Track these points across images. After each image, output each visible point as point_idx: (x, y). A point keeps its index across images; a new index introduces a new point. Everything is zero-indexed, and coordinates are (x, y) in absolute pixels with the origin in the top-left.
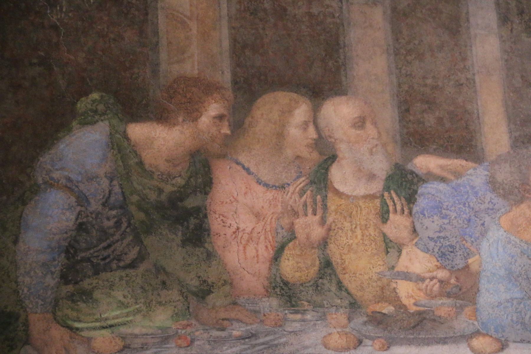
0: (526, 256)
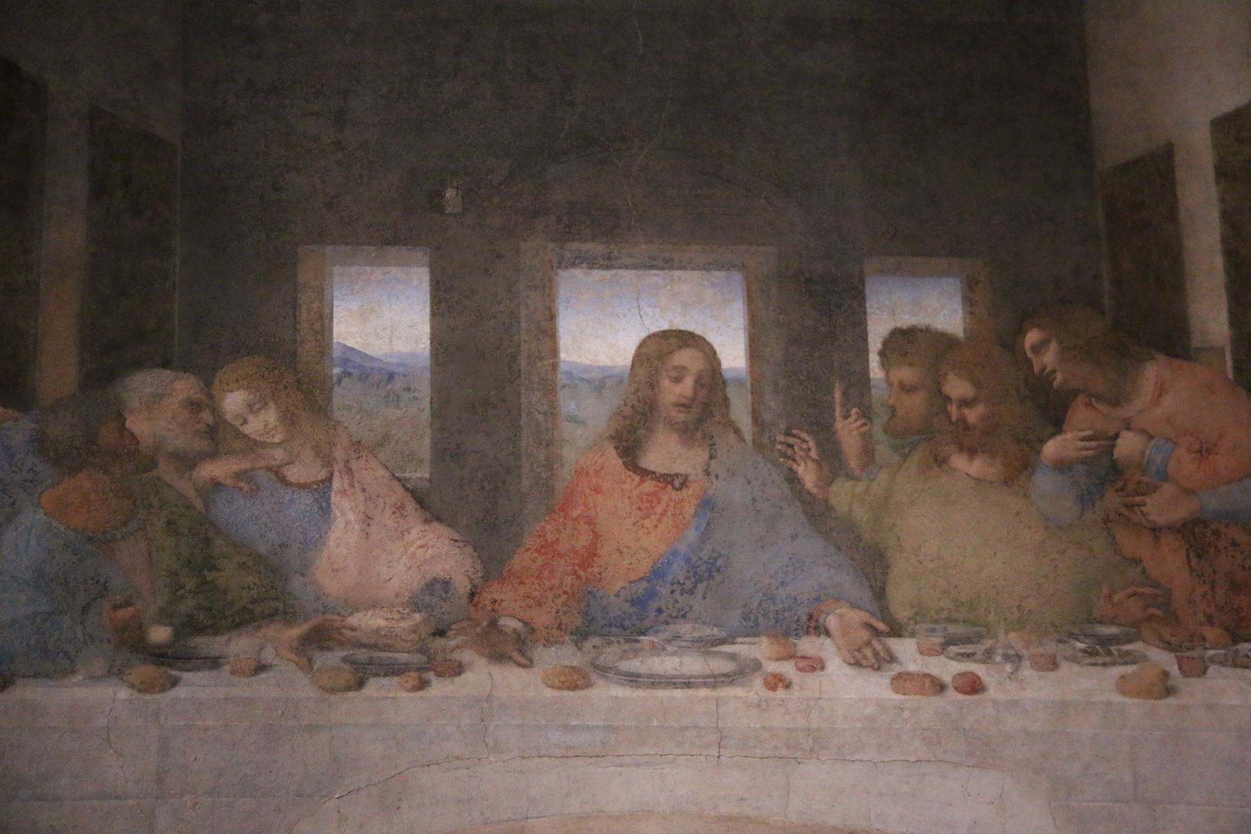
0: (70, 550)
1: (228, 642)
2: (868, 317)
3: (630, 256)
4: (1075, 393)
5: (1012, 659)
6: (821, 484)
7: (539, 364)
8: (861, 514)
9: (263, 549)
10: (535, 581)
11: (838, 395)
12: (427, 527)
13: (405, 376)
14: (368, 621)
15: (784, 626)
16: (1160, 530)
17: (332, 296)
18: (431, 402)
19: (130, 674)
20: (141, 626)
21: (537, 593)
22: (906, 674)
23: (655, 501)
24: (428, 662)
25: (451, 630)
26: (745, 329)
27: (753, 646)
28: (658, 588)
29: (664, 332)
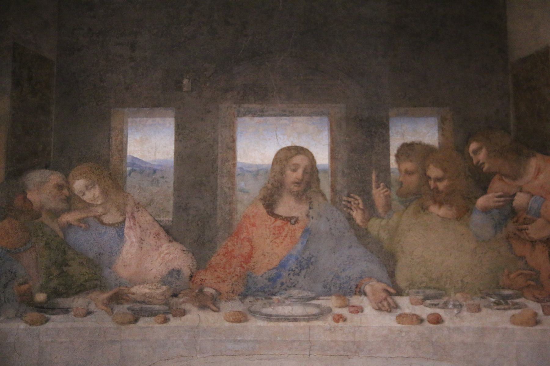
1: (73, 301)
2: (390, 138)
3: (273, 110)
4: (494, 174)
5: (457, 307)
6: (364, 221)
7: (227, 164)
8: (384, 236)
9: (91, 255)
10: (222, 270)
11: (374, 177)
12: (170, 244)
13: (161, 171)
14: (140, 290)
16: (536, 241)
17: (127, 133)
18: (174, 183)
19: (26, 317)
20: (32, 293)
21: (223, 276)
22: (404, 314)
23: (282, 230)
24: (169, 310)
25: (180, 294)
26: (328, 145)
27: (328, 301)
28: (282, 272)
29: (288, 147)
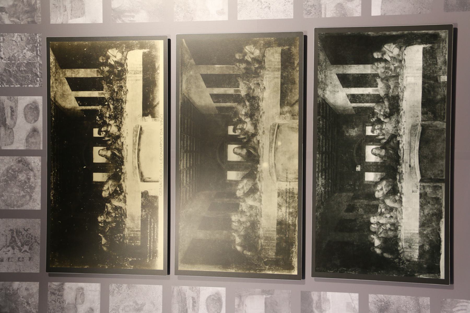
15: (58, 309)
